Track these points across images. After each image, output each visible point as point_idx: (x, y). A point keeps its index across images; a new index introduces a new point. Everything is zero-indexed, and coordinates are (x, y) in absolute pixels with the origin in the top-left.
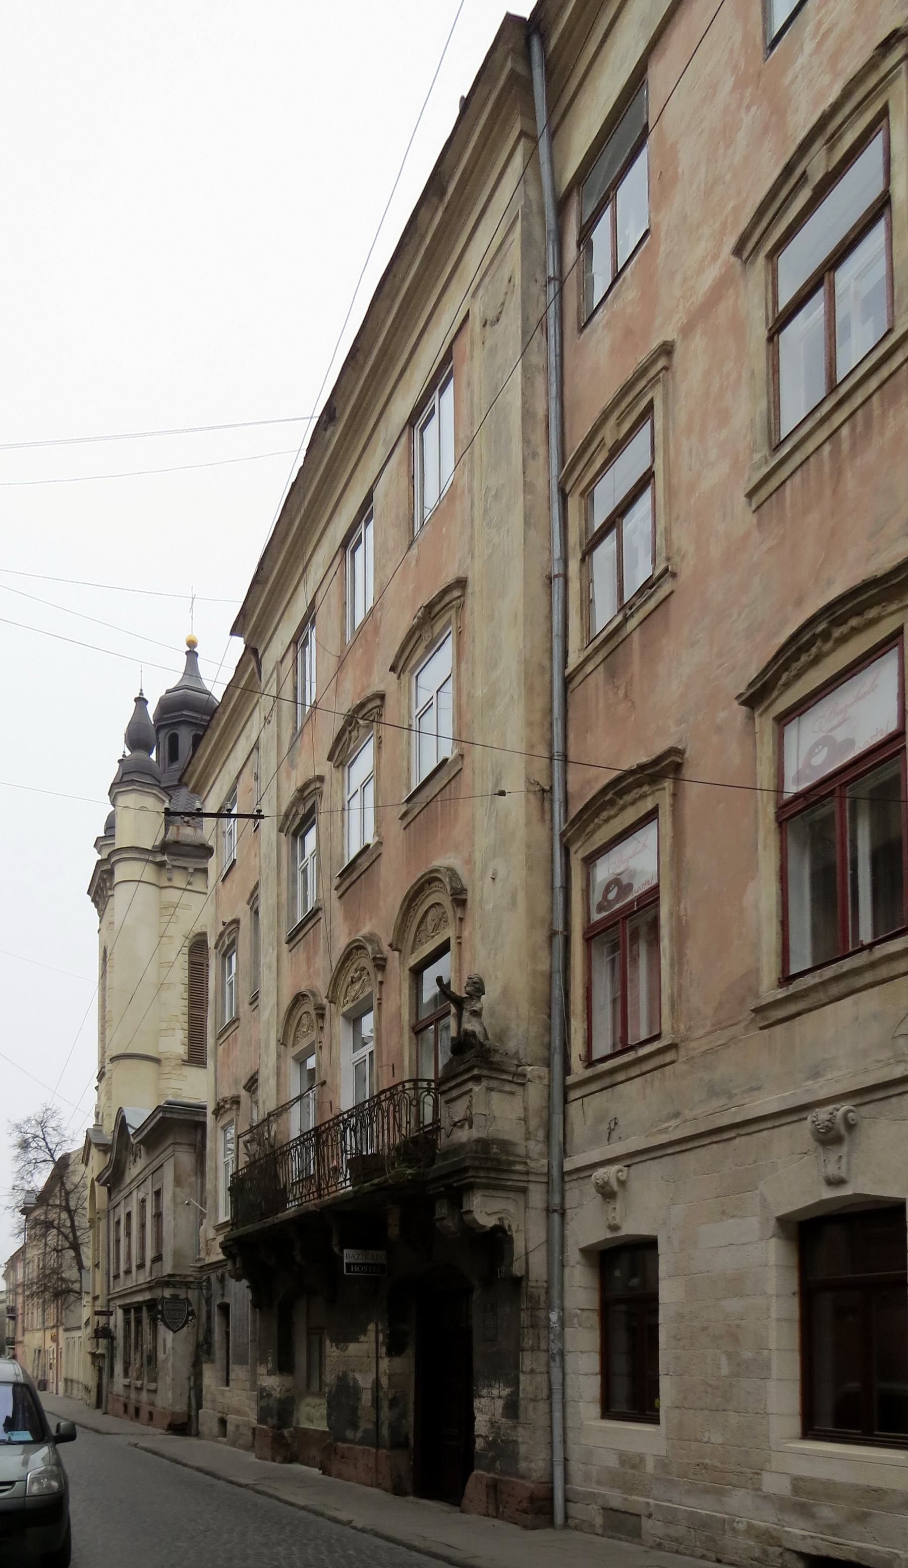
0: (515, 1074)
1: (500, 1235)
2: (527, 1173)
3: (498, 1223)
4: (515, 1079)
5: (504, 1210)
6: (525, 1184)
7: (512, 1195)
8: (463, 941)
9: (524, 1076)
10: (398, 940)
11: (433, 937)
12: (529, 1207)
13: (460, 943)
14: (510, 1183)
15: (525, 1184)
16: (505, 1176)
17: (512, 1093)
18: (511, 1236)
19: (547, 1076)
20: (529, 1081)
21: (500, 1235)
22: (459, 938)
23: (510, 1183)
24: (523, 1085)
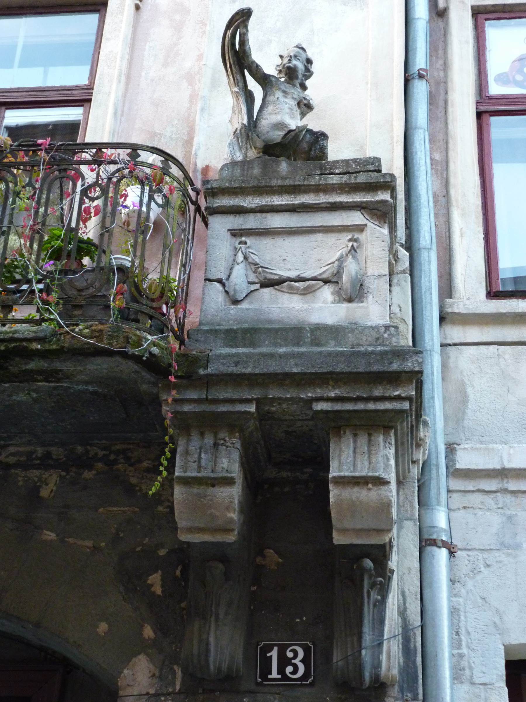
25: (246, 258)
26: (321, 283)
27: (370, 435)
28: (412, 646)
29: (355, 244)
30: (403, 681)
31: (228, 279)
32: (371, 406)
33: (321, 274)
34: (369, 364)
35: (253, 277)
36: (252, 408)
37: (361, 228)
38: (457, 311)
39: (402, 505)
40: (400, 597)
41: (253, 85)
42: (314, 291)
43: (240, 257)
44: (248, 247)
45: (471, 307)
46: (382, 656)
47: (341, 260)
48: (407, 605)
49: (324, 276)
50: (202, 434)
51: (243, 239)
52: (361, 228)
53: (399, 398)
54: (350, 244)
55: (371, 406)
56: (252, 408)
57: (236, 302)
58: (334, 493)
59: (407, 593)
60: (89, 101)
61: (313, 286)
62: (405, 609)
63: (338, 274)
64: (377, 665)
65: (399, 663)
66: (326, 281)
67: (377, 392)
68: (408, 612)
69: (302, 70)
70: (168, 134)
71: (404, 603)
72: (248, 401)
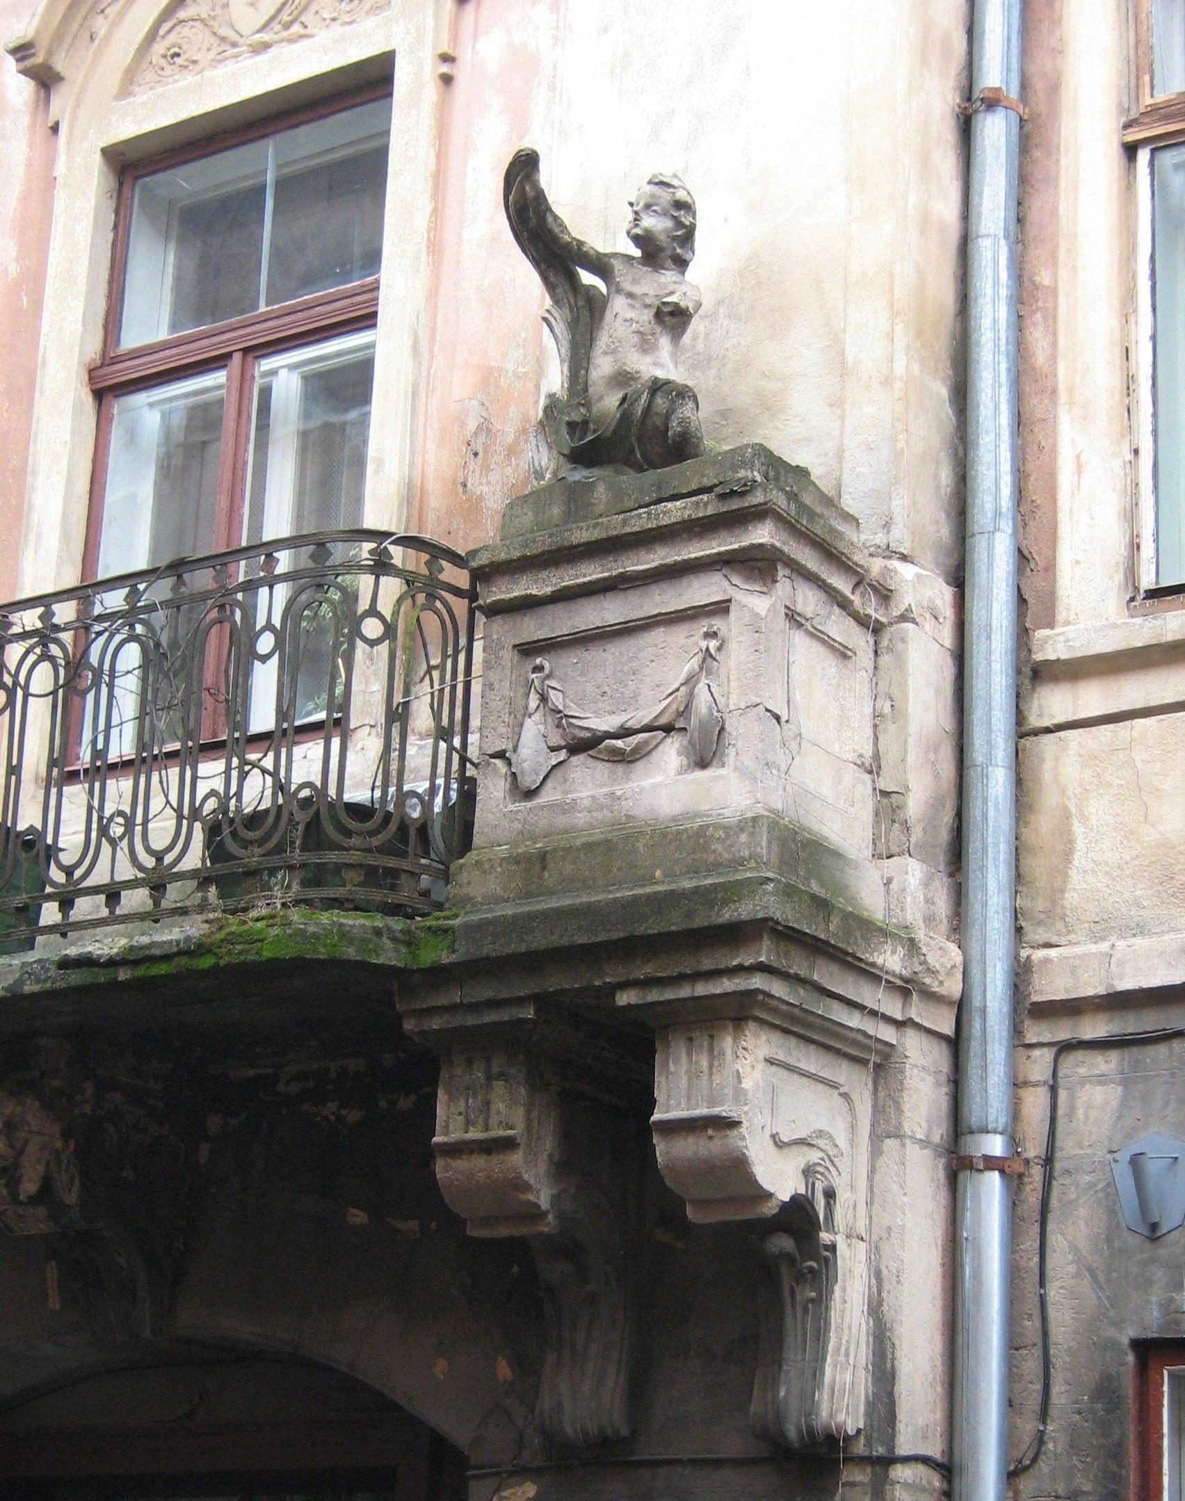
0: (860, 579)
1: (783, 1243)
2: (905, 988)
3: (802, 1191)
4: (856, 599)
5: (820, 1134)
6: (887, 1034)
7: (843, 1073)
8: (461, 72)
9: (885, 595)
10: (58, 36)
11: (266, 46)
12: (898, 1135)
13: (447, 80)
14: (854, 1020)
15: (887, 1034)
16: (827, 975)
17: (843, 653)
18: (833, 1248)
19: (948, 612)
20: (904, 618)
21: (783, 1243)
22: (447, 58)
23: (854, 1020)
24: (877, 629)
25: (544, 699)
26: (661, 734)
27: (712, 1037)
28: (889, 1365)
29: (713, 644)
30: (872, 1426)
31: (515, 749)
32: (701, 989)
33: (656, 718)
34: (689, 914)
35: (556, 740)
36: (529, 1013)
37: (722, 608)
38: (1052, 657)
39: (881, 1109)
40: (874, 1281)
41: (587, 278)
42: (649, 752)
43: (533, 701)
44: (548, 677)
45: (1077, 644)
46: (821, 1395)
47: (691, 680)
48: (884, 1294)
49: (663, 721)
50: (470, 1062)
51: (538, 661)
52: (722, 608)
53: (740, 969)
54: (704, 644)
55: (701, 989)
56: (529, 1013)
57: (530, 794)
58: (663, 1149)
59: (884, 1271)
60: (374, 315)
61: (646, 742)
62: (880, 1302)
63: (685, 712)
64: (811, 1407)
65: (866, 1397)
66: (668, 729)
67: (707, 964)
68: (885, 1308)
69: (666, 230)
70: (511, 367)
71: (879, 1293)
72: (520, 1001)
